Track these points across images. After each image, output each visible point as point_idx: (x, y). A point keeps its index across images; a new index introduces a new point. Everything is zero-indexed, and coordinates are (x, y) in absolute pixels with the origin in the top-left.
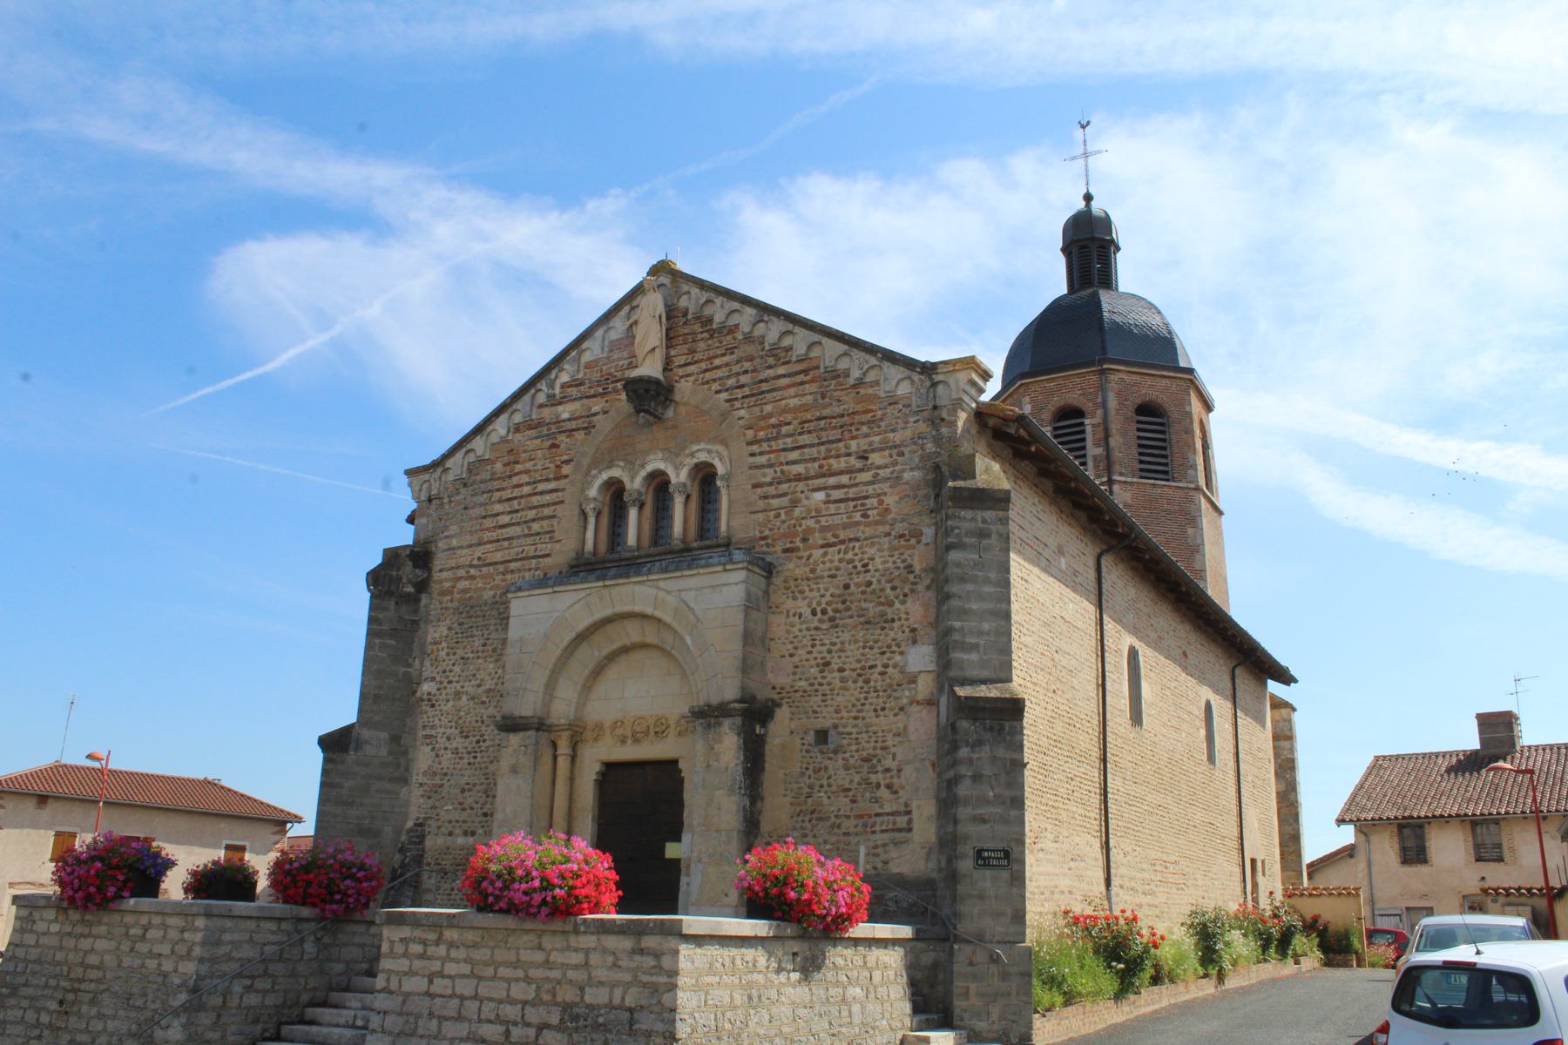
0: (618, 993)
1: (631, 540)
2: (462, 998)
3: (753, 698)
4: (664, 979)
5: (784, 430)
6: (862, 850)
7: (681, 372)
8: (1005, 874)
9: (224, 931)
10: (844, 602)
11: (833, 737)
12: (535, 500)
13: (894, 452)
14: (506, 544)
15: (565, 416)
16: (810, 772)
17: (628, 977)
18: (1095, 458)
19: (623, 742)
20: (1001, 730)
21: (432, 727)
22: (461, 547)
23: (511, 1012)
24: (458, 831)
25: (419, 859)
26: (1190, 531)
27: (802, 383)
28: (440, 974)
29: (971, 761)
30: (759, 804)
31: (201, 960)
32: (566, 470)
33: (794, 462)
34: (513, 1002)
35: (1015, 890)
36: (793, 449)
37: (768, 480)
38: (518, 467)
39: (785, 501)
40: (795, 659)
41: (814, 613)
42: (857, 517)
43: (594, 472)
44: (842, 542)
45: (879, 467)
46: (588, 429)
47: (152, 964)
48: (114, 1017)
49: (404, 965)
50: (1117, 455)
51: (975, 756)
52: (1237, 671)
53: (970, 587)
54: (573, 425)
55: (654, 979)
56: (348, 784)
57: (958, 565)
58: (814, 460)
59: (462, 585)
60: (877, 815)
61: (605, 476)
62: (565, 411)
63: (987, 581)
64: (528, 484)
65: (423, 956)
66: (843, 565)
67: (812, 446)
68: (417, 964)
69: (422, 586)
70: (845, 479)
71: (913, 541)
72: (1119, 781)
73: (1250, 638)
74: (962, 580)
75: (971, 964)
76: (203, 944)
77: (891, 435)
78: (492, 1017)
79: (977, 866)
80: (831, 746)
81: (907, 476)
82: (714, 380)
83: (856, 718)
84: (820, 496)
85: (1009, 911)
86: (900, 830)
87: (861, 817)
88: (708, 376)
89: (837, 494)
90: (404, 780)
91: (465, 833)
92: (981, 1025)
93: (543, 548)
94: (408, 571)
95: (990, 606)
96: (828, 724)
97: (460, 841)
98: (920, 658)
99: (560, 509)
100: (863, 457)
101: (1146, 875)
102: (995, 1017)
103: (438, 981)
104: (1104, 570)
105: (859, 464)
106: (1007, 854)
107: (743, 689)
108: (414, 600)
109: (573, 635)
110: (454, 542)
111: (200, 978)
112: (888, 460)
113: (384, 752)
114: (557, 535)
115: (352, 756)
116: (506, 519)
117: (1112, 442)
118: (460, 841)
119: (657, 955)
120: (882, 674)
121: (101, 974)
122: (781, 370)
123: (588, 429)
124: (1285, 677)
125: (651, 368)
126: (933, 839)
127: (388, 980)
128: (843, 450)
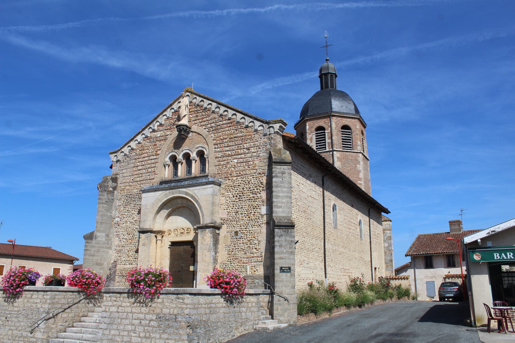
0: (172, 310)
1: (179, 174)
2: (128, 313)
3: (216, 222)
4: (185, 306)
5: (224, 141)
6: (248, 267)
8: (289, 274)
9: (56, 295)
10: (242, 193)
11: (240, 235)
12: (149, 161)
13: (257, 148)
14: (140, 175)
15: (159, 135)
16: (233, 244)
17: (175, 306)
18: (328, 143)
19: (177, 236)
20: (288, 232)
21: (119, 232)
23: (142, 316)
24: (127, 263)
26: (358, 166)
27: (230, 127)
28: (121, 306)
29: (279, 241)
30: (218, 254)
31: (50, 304)
32: (159, 152)
33: (228, 151)
35: (292, 279)
36: (227, 147)
37: (220, 156)
38: (144, 152)
39: (225, 162)
40: (228, 210)
41: (234, 197)
42: (247, 167)
44: (242, 175)
45: (253, 153)
47: (34, 305)
48: (23, 322)
49: (110, 303)
50: (335, 142)
51: (280, 239)
52: (371, 210)
53: (279, 189)
54: (161, 138)
55: (182, 306)
56: (93, 249)
57: (276, 182)
60: (252, 257)
61: (171, 154)
62: (158, 134)
63: (285, 187)
64: (147, 157)
65: (115, 301)
66: (242, 182)
67: (233, 146)
68: (115, 303)
69: (115, 188)
70: (243, 156)
71: (263, 175)
72: (330, 245)
73: (374, 200)
74: (277, 187)
75: (279, 301)
76: (50, 299)
77: (256, 143)
78: (136, 317)
79: (281, 272)
80: (239, 237)
81: (261, 155)
82: (204, 125)
83: (246, 228)
84: (236, 161)
85: (290, 285)
86: (259, 262)
88: (202, 123)
90: (110, 248)
91: (129, 264)
92: (282, 318)
93: (152, 177)
94: (110, 184)
95: (286, 194)
96: (238, 230)
97: (128, 266)
101: (338, 273)
102: (286, 316)
103: (120, 308)
104: (325, 180)
105: (247, 152)
106: (290, 268)
107: (212, 219)
108: (112, 193)
109: (161, 203)
110: (125, 175)
111: (49, 309)
112: (256, 150)
113: (104, 239)
114: (156, 173)
115: (94, 241)
117: (333, 138)
118: (128, 266)
119: (183, 299)
120: (254, 215)
121: (18, 309)
122: (224, 122)
124: (387, 212)
125: (184, 121)
126: (269, 264)
128: (242, 147)
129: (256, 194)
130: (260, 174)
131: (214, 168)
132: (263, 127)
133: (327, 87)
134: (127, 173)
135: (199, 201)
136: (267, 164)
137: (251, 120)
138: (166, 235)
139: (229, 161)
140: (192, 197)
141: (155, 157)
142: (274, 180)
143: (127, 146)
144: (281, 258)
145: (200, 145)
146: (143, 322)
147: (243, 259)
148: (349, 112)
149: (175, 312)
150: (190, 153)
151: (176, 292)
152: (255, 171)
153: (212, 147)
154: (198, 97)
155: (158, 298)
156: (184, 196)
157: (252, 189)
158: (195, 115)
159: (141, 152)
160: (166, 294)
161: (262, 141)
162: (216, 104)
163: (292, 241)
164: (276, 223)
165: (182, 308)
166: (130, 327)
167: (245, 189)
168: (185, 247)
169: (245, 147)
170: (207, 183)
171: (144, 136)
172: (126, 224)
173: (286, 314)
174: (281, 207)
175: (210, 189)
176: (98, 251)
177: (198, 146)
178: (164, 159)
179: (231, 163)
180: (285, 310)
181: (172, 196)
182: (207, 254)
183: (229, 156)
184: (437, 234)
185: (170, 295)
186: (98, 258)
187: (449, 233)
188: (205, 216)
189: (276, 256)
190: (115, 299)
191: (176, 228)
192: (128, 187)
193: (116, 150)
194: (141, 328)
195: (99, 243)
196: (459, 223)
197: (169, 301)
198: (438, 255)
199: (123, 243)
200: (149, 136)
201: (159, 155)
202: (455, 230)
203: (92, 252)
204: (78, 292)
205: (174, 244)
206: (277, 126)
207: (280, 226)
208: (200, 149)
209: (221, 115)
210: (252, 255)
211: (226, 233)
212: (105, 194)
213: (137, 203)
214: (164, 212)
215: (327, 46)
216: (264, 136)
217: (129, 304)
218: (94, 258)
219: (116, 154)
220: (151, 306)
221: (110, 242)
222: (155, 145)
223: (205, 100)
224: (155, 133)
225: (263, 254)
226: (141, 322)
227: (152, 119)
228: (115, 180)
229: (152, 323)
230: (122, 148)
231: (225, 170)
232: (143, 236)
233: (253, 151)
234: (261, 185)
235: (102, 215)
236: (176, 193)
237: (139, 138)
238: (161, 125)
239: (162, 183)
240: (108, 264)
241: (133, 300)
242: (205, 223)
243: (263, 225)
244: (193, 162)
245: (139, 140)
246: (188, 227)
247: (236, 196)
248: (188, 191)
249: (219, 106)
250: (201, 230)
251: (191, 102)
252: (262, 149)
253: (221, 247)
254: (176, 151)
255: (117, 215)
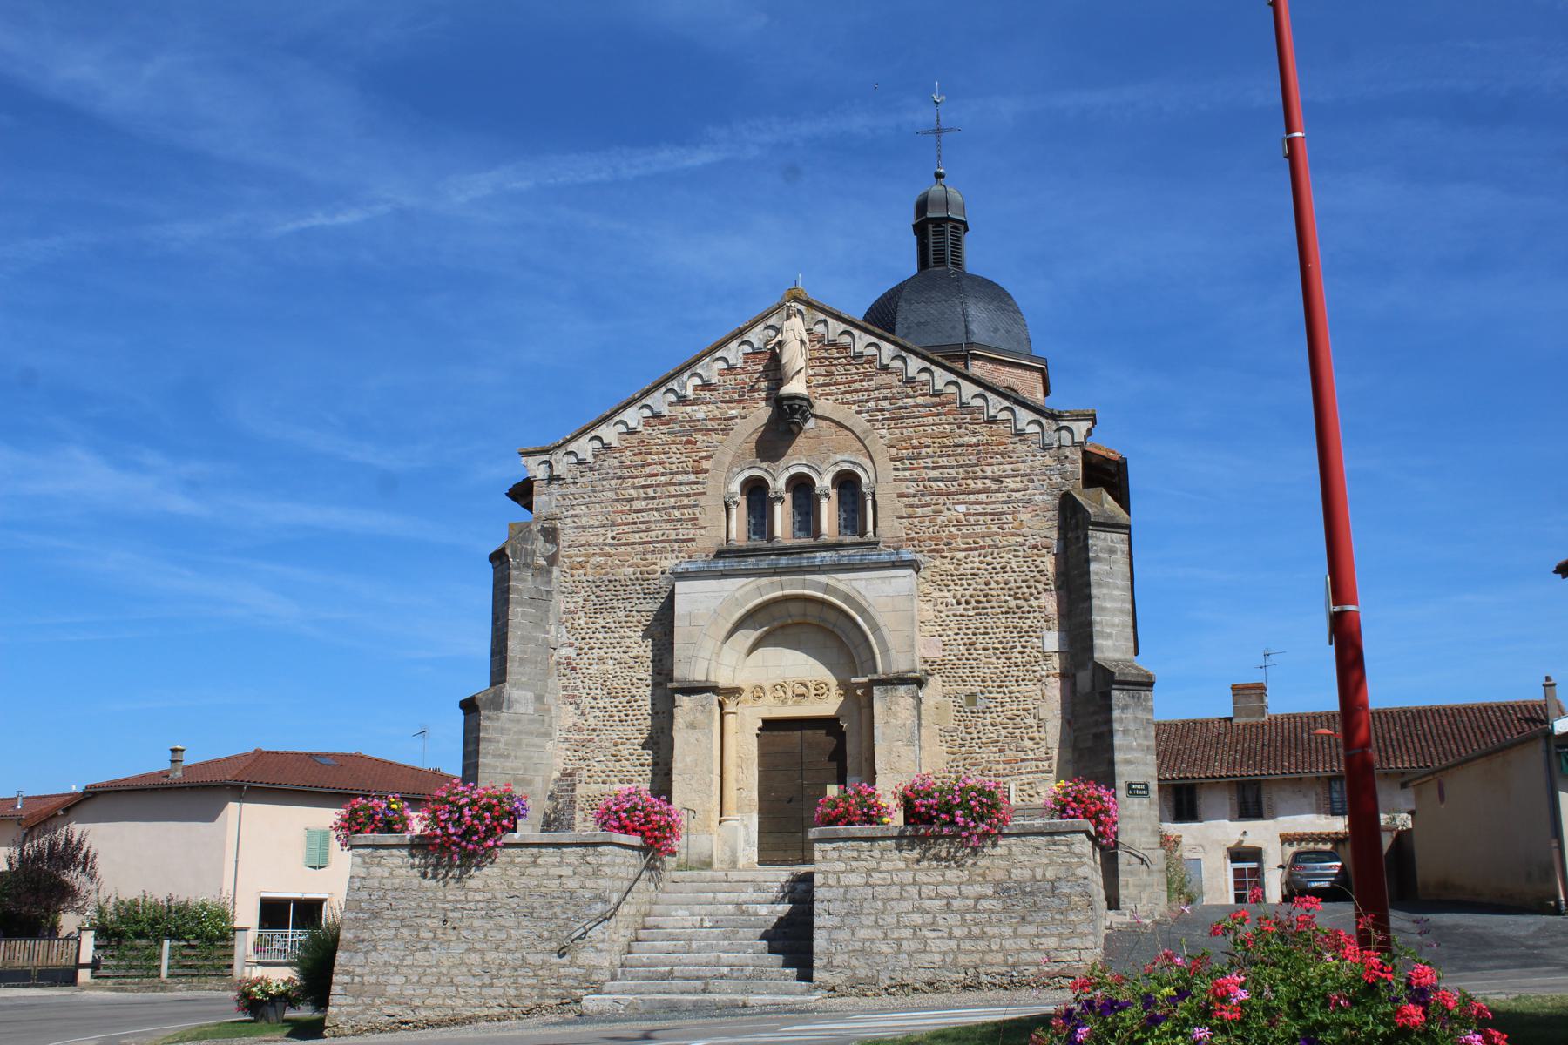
2: (902, 885)
4: (1075, 860)
5: (924, 451)
7: (819, 390)
11: (982, 703)
12: (672, 489)
14: (643, 527)
15: (701, 415)
17: (1045, 861)
19: (784, 702)
21: (576, 688)
22: (592, 527)
23: (950, 890)
25: (572, 804)
28: (875, 870)
29: (1121, 720)
32: (706, 464)
33: (936, 480)
34: (950, 883)
36: (933, 468)
37: (912, 491)
38: (649, 459)
41: (959, 603)
42: (995, 529)
43: (736, 470)
44: (983, 548)
46: (726, 431)
49: (841, 866)
53: (1105, 591)
54: (710, 425)
56: (504, 738)
58: (955, 479)
59: (592, 560)
61: (747, 474)
62: (700, 412)
64: (663, 474)
65: (855, 859)
69: (552, 560)
70: (983, 497)
74: (1100, 585)
77: (1021, 466)
78: (933, 894)
79: (1129, 795)
82: (854, 402)
84: (962, 508)
87: (1009, 762)
88: (848, 396)
89: (979, 508)
90: (548, 735)
94: (540, 545)
95: (1119, 605)
96: (977, 690)
97: (617, 787)
98: (1052, 641)
99: (702, 500)
100: (998, 480)
103: (876, 876)
108: (545, 572)
109: (743, 611)
110: (584, 521)
112: (1020, 485)
114: (701, 523)
115: (504, 714)
116: (643, 504)
122: (920, 400)
123: (726, 431)
127: (826, 878)
129: (1026, 600)
130: (1035, 547)
131: (896, 523)
132: (1041, 425)
133: (940, 261)
134: (593, 516)
135: (871, 610)
136: (1055, 523)
137: (1006, 403)
138: (746, 701)
139: (940, 507)
140: (847, 598)
141: (692, 477)
142: (1093, 567)
143: (588, 436)
144: (1128, 762)
145: (846, 457)
146: (956, 904)
147: (995, 766)
148: (1014, 346)
149: (1050, 874)
150: (814, 475)
151: (1048, 829)
152: (1020, 539)
153: (885, 466)
154: (831, 321)
155: (995, 845)
156: (820, 595)
157: (1012, 585)
158: (822, 370)
159: (638, 458)
160: (1018, 835)
161: (1037, 463)
162: (892, 347)
163: (1148, 721)
164: (1117, 677)
165: (1069, 865)
166: (917, 919)
167: (993, 585)
168: (808, 733)
169: (989, 473)
170: (894, 565)
171: (647, 413)
172: (602, 667)
173: (1145, 896)
174: (1109, 636)
175: (903, 580)
176: (518, 744)
177: (839, 457)
178: (726, 485)
179: (946, 513)
180: (1143, 887)
181: (779, 593)
182: (904, 751)
183: (940, 493)
184: (1195, 722)
185: (1030, 838)
186: (518, 764)
187: (1230, 719)
188: (893, 652)
189: (1118, 756)
190: (855, 854)
191: (780, 681)
192: (601, 560)
193: (548, 445)
194: (953, 919)
195: (519, 721)
196: (1259, 690)
197: (1029, 850)
198: (1214, 783)
199: (592, 721)
200: (665, 411)
201: (706, 471)
202: (1250, 712)
203: (501, 746)
204: (638, 848)
205: (769, 725)
206: (1081, 428)
207: (1125, 684)
208: (846, 466)
209: (910, 381)
210: (1022, 755)
211: (939, 698)
212: (528, 574)
213: (640, 608)
214: (748, 636)
215: (938, 131)
216: (1044, 449)
217: (902, 865)
218: (509, 764)
219: (546, 458)
220: (974, 864)
221: (547, 719)
222: (688, 442)
223: (856, 332)
224: (688, 409)
225: (1055, 753)
226: (948, 904)
227: (677, 365)
228: (551, 535)
229: (985, 904)
230: (567, 441)
231: (928, 530)
232: (684, 702)
233: (1012, 486)
234: (1038, 576)
235: (522, 637)
236: (794, 586)
237: (632, 416)
238: (707, 385)
239: (720, 555)
240: (546, 781)
241: (916, 853)
242: (894, 669)
243: (1051, 679)
244: (824, 501)
245: (632, 424)
246: (820, 679)
247: (967, 603)
248: (832, 582)
249: (904, 354)
250: (882, 688)
251: (809, 332)
252: (1037, 484)
253: (929, 733)
254: (765, 465)
255: (564, 640)
